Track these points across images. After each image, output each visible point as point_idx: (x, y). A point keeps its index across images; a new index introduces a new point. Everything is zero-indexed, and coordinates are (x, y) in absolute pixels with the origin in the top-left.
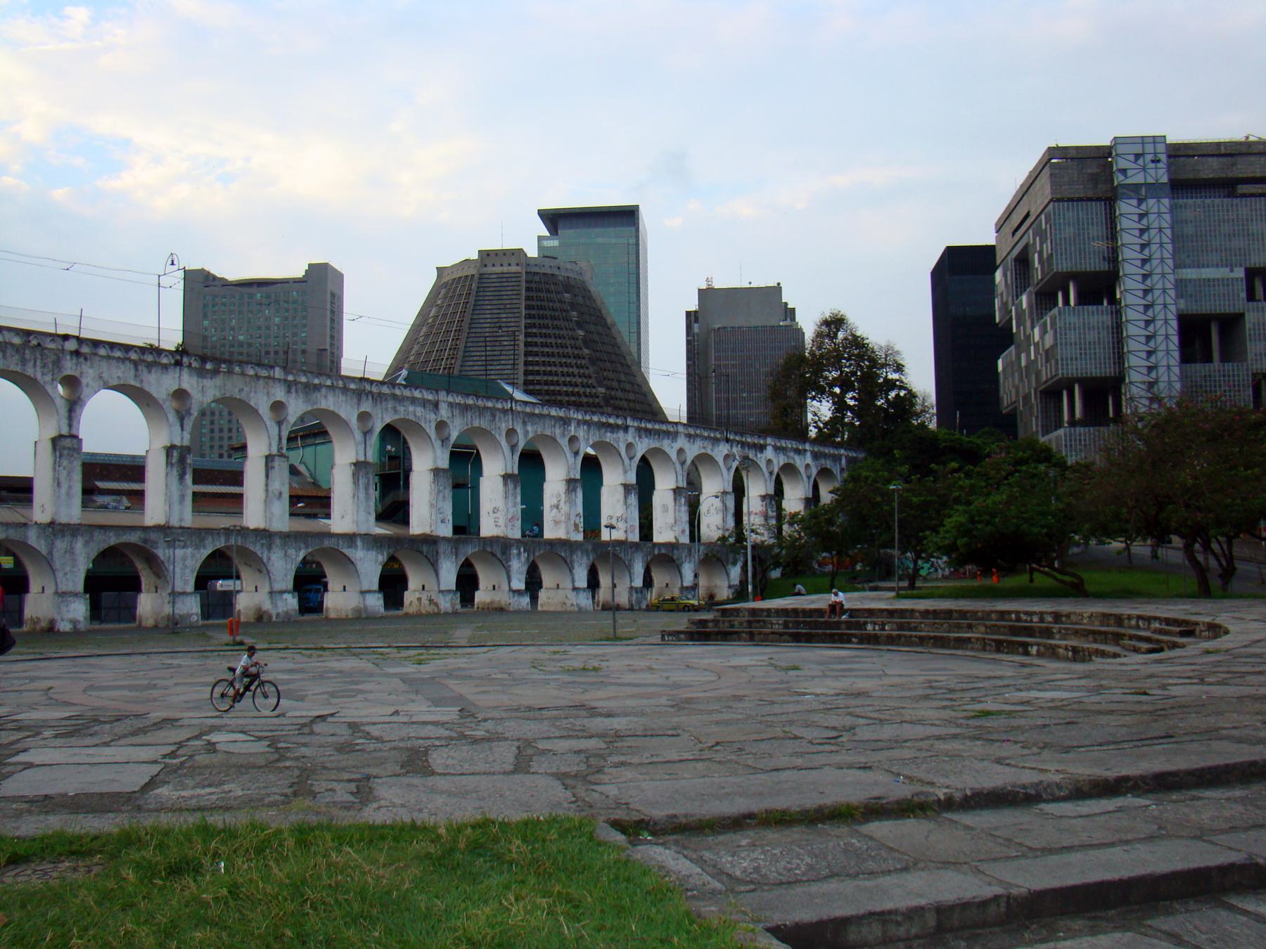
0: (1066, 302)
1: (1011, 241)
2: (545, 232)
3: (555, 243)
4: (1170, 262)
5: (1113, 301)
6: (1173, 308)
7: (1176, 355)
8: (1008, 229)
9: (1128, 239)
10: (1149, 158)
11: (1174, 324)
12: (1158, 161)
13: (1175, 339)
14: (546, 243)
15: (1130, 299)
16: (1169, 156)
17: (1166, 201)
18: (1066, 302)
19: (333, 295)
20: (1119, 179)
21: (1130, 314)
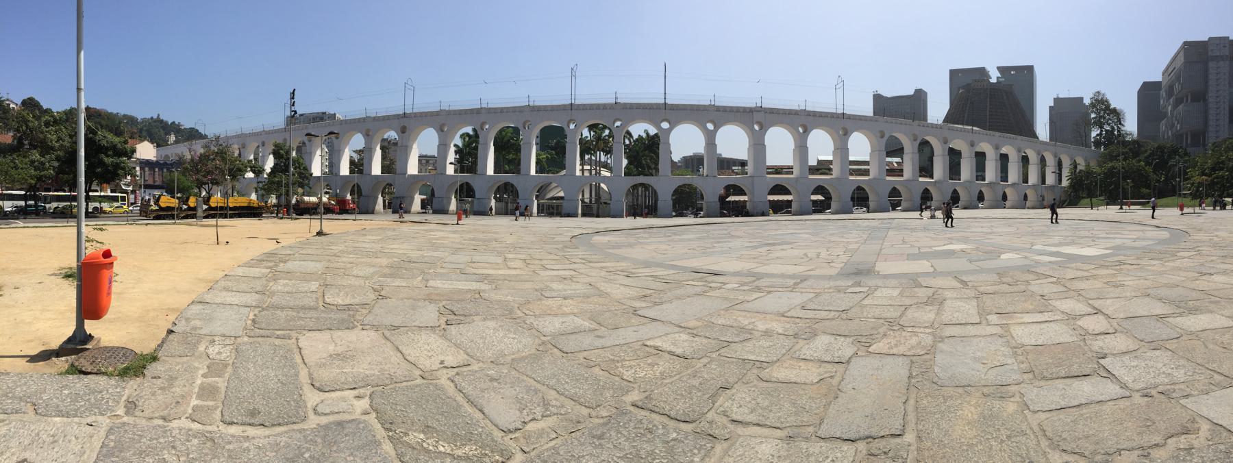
0: (1187, 101)
1: (1167, 79)
2: (999, 75)
3: (1003, 80)
4: (1227, 86)
5: (1205, 100)
6: (1227, 103)
7: (1227, 120)
8: (1166, 75)
9: (1212, 77)
10: (1222, 45)
11: (1227, 109)
12: (1226, 47)
13: (1228, 115)
14: (1001, 80)
15: (1211, 100)
16: (1230, 45)
17: (1228, 62)
18: (1187, 101)
19: (923, 100)
20: (1210, 53)
21: (1211, 105)
